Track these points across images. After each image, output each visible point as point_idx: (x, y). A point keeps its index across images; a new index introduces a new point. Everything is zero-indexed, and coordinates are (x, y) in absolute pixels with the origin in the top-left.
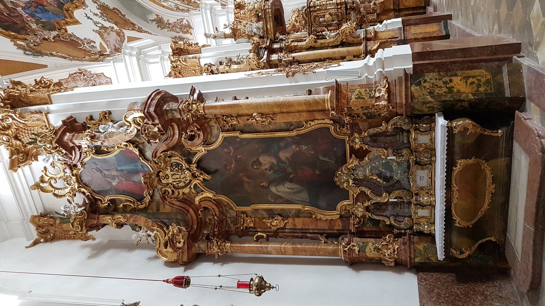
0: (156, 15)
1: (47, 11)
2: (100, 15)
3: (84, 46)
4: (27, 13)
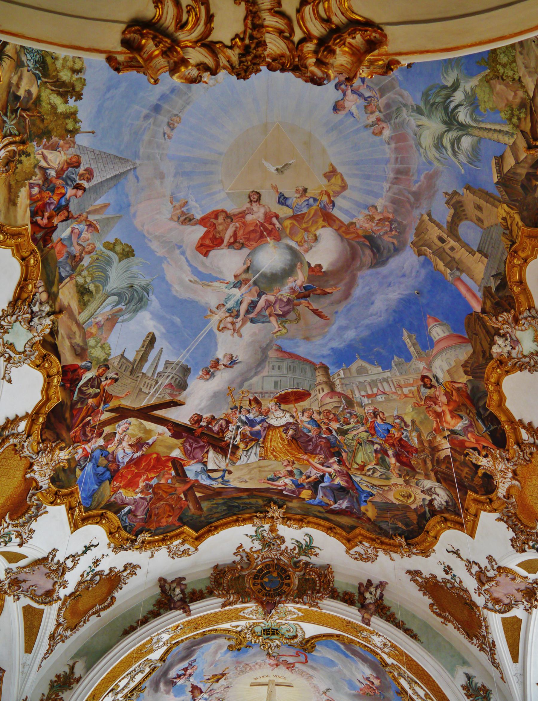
0: (80, 678)
1: (100, 483)
2: (97, 569)
3: (9, 524)
4: (93, 452)
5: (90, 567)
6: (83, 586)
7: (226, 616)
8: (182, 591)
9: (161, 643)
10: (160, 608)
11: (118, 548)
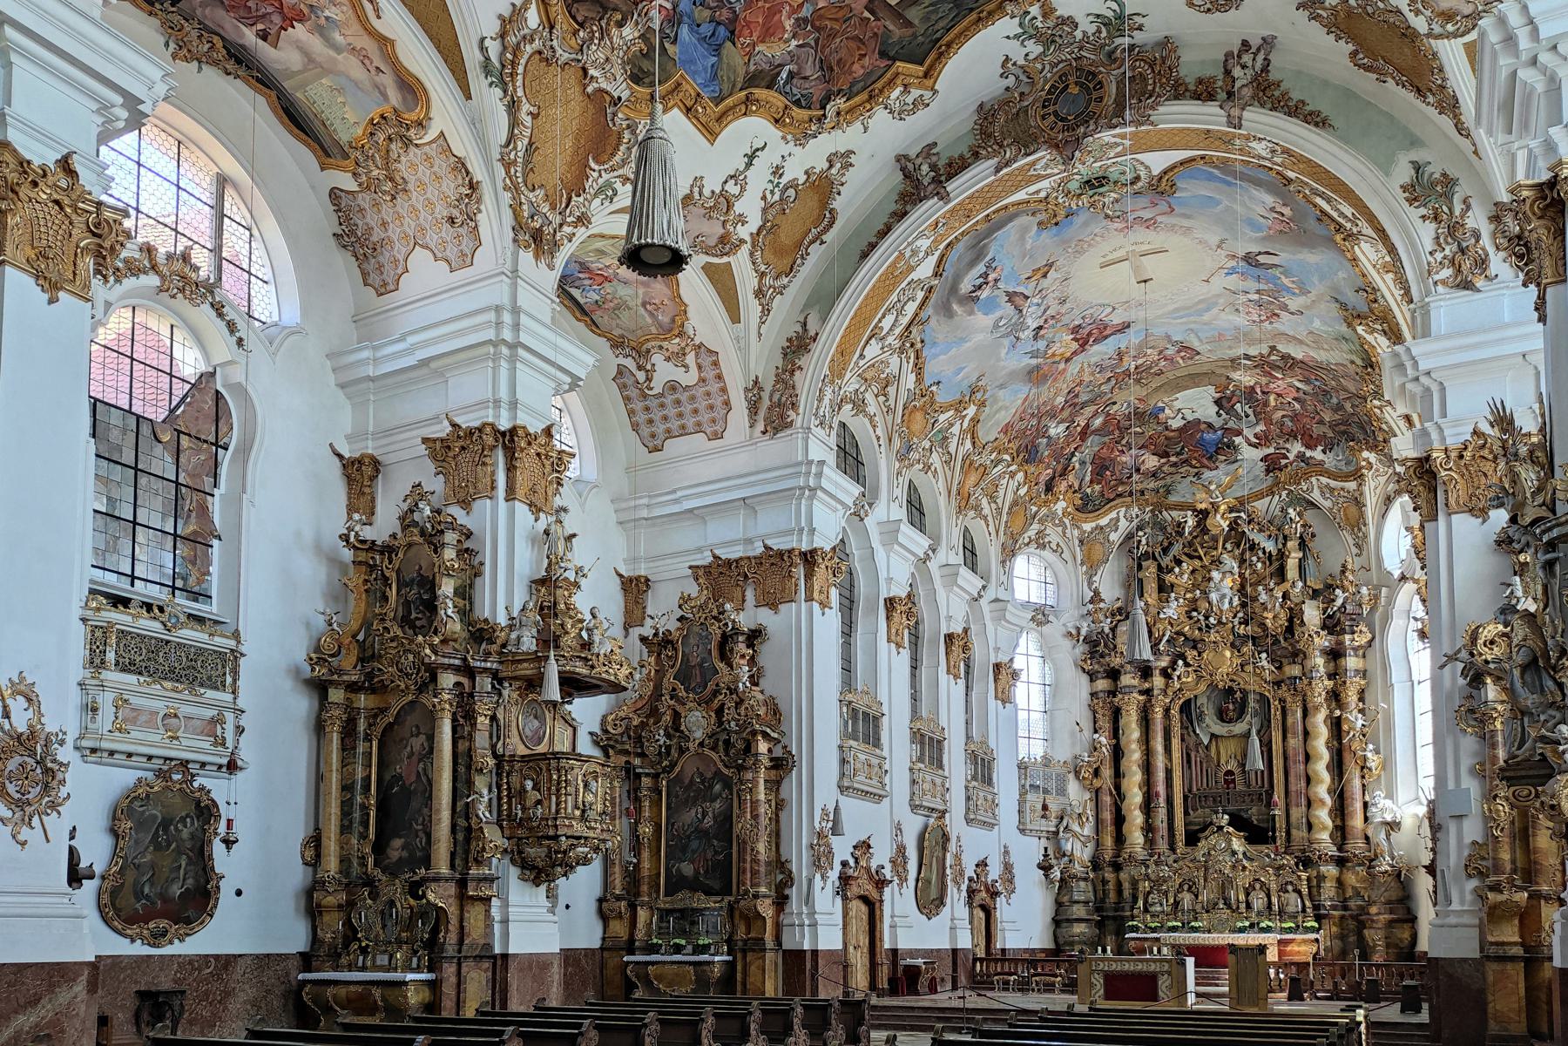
5: (771, 181)
6: (773, 211)
7: (1010, 183)
8: (933, 167)
9: (921, 255)
10: (906, 203)
11: (802, 138)
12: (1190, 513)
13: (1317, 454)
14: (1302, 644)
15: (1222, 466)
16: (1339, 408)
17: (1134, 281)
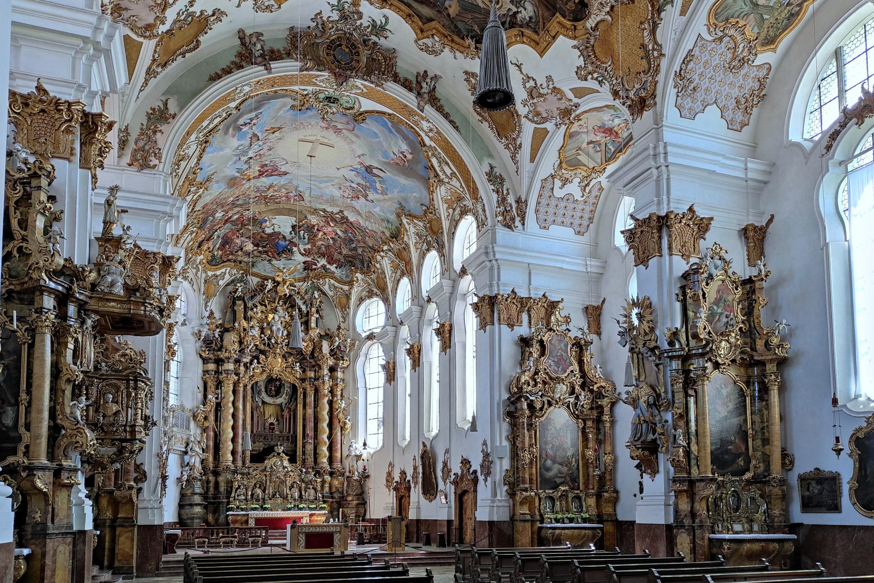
12: (270, 281)
13: (333, 268)
14: (321, 361)
15: (283, 260)
16: (355, 249)
17: (307, 154)
